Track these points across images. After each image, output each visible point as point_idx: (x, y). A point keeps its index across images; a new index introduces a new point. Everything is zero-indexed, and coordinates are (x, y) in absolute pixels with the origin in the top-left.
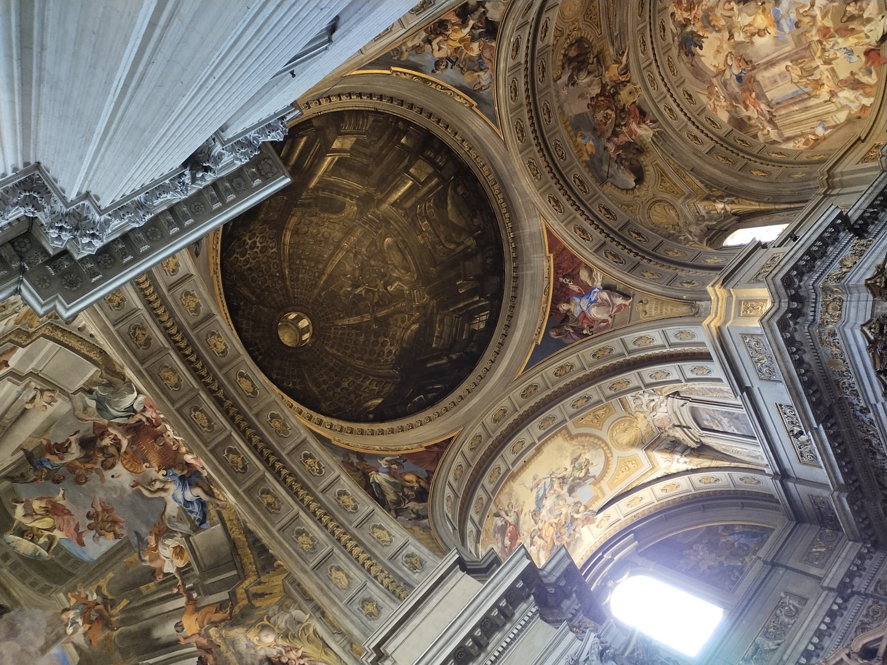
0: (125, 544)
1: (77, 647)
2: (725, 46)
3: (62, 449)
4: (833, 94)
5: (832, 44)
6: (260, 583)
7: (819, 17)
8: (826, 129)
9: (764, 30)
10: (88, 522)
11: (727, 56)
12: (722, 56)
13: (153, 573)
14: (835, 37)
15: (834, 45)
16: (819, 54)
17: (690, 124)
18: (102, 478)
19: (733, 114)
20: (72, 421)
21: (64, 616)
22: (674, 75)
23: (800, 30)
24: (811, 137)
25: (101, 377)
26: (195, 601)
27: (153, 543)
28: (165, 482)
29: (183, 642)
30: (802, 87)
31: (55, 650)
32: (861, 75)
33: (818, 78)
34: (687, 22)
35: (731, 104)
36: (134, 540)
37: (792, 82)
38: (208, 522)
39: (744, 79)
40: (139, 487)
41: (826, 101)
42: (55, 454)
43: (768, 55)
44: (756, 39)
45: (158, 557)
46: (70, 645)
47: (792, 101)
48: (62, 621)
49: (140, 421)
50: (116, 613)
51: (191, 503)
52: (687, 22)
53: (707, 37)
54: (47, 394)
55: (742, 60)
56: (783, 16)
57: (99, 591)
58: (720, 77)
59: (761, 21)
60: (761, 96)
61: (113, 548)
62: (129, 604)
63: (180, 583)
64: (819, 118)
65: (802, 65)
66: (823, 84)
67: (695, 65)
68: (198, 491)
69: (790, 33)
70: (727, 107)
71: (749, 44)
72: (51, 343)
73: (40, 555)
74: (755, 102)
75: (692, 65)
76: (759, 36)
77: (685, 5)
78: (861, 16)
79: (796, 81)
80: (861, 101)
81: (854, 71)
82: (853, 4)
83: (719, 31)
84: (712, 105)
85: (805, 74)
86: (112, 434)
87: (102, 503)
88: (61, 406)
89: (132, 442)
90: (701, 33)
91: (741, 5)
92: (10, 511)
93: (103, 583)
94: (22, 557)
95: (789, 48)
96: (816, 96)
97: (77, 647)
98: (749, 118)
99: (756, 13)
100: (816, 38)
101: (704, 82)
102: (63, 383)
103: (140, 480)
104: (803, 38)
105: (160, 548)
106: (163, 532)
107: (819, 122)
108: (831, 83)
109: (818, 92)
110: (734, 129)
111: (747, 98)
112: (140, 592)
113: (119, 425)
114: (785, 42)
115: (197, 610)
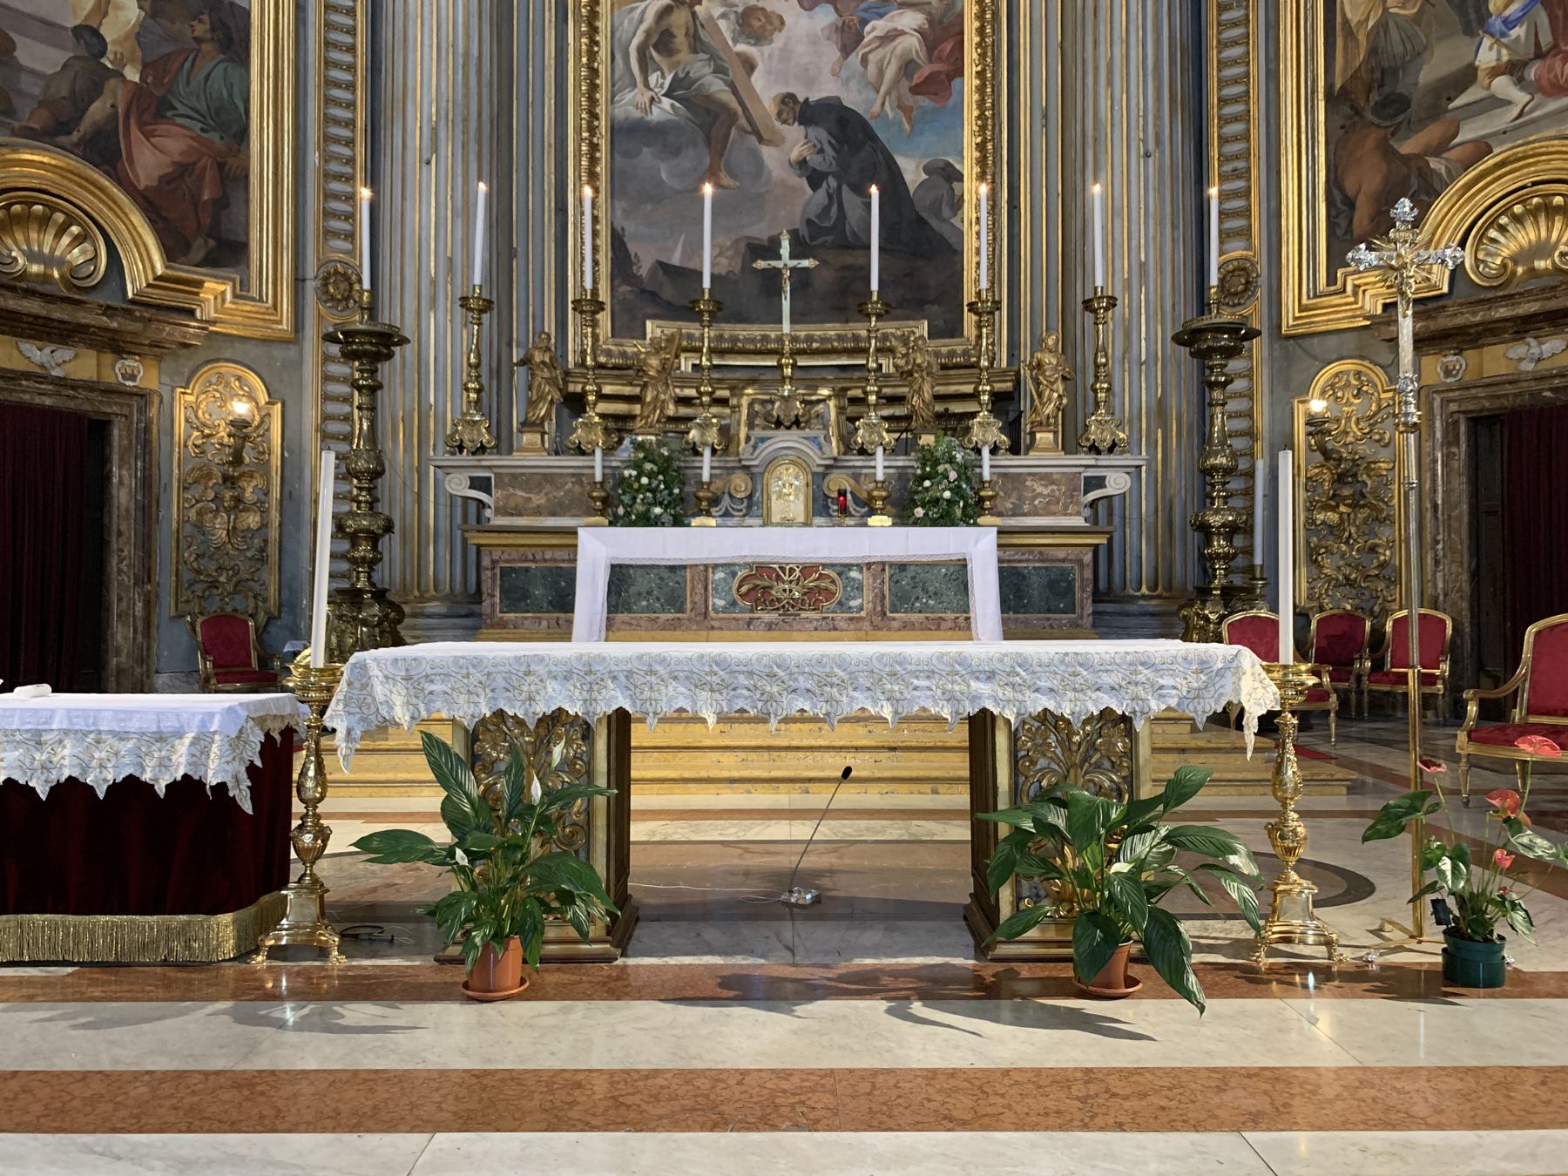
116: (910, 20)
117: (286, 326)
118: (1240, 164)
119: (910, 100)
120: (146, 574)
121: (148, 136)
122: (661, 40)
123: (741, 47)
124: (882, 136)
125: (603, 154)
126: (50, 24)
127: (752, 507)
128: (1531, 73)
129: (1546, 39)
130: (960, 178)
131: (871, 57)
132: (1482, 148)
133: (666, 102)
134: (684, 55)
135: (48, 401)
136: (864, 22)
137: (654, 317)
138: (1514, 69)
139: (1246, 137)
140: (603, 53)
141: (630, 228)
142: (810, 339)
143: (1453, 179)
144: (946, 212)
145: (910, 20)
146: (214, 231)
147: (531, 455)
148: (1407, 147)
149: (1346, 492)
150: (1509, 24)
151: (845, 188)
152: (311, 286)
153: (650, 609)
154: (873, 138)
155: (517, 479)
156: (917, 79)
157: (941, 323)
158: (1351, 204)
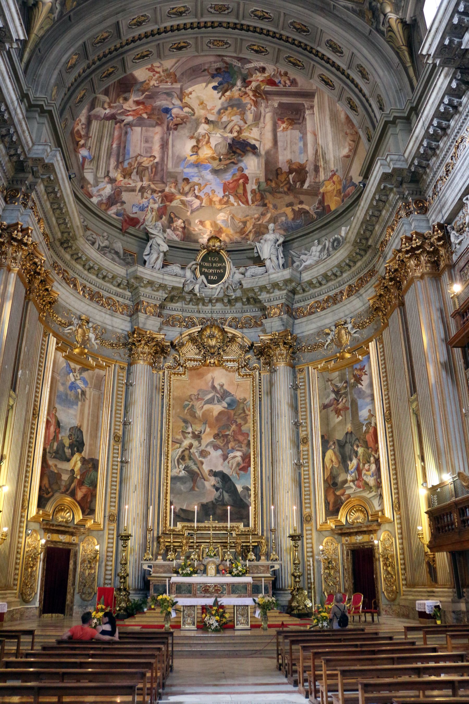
2: (202, 112)
4: (112, 181)
5: (157, 199)
7: (184, 198)
8: (84, 158)
9: (197, 152)
11: (193, 110)
12: (195, 104)
14: (161, 203)
15: (154, 200)
16: (152, 186)
17: (155, 27)
19: (138, 86)
22: (210, 42)
23: (180, 181)
24: (82, 142)
30: (130, 161)
32: (119, 208)
33: (133, 177)
34: (246, 83)
35: (148, 90)
37: (139, 155)
39: (163, 115)
41: (108, 172)
43: (173, 146)
44: (193, 143)
47: (122, 145)
52: (246, 83)
53: (220, 98)
55: (181, 122)
56: (200, 172)
58: (178, 93)
59: (206, 152)
60: (140, 122)
64: (96, 158)
65: (150, 170)
66: (125, 178)
67: (204, 73)
69: (183, 171)
70: (148, 84)
71: (192, 134)
74: (138, 114)
75: (205, 70)
76: (194, 146)
77: (263, 87)
78: (169, 227)
79: (139, 158)
80: (97, 197)
81: (125, 206)
82: (183, 225)
83: (219, 112)
84: (158, 70)
85: (141, 168)
90: (228, 93)
91: (229, 141)
95: (170, 166)
96: (117, 167)
98: (126, 99)
99: (215, 151)
100: (167, 190)
101: (182, 74)
104: (172, 180)
107: (92, 157)
108: (122, 183)
109: (119, 171)
110: (125, 75)
111: (146, 108)
114: (177, 165)
116: (239, 454)
117: (102, 527)
118: (308, 493)
119: (239, 472)
120: (74, 584)
121: (80, 489)
122: (182, 458)
123: (200, 459)
124: (233, 480)
125: (169, 485)
126: (67, 470)
127: (205, 571)
128: (356, 482)
129: (357, 477)
130: (250, 490)
131: (230, 462)
132: (349, 496)
133: (183, 472)
134: (187, 461)
135: (61, 547)
136: (228, 454)
137: (179, 521)
138: (353, 481)
139: (309, 487)
140: (169, 461)
141: (174, 501)
142: (216, 527)
143: (345, 501)
144: (247, 498)
145: (239, 454)
146: (89, 508)
147: (160, 561)
148: (338, 493)
149: (330, 565)
150: (352, 472)
151: (224, 492)
152: (107, 518)
153: (185, 593)
154: (230, 480)
155: (157, 566)
156: (240, 467)
157: (246, 523)
158: (329, 503)
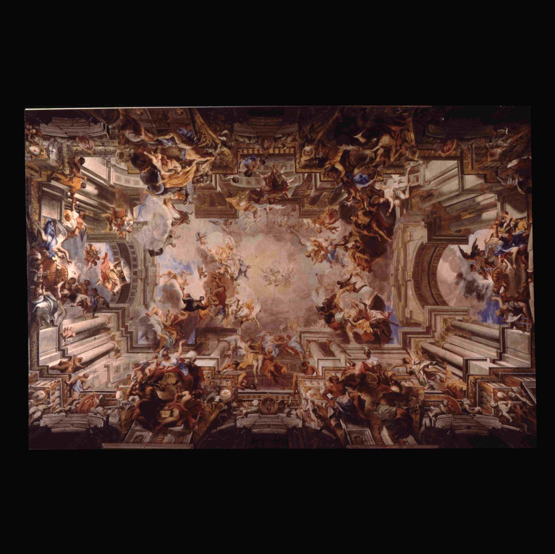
0: (91, 239)
1: (132, 213)
3: (82, 304)
6: (32, 175)
10: (98, 262)
13: (84, 217)
18: (79, 277)
20: (69, 313)
21: (131, 230)
25: (42, 325)
26: (70, 191)
27: (77, 231)
28: (56, 253)
29: (86, 178)
31: (142, 220)
36: (85, 238)
38: (47, 220)
40: (68, 260)
42: (87, 304)
45: (78, 223)
46: (135, 216)
48: (133, 228)
49: (46, 291)
50: (109, 214)
51: (50, 234)
54: (64, 335)
57: (111, 229)
61: (96, 242)
62: (100, 213)
63: (74, 204)
68: (44, 237)
72: (41, 359)
73: (124, 263)
86: (62, 295)
87: (87, 265)
88: (67, 324)
89: (56, 283)
92: (120, 292)
93: (107, 230)
94: (130, 268)
97: (132, 213)
102: (55, 336)
103: (66, 263)
105: (75, 226)
106: (71, 233)
112: (94, 214)
113: (55, 296)
115: (70, 187)
